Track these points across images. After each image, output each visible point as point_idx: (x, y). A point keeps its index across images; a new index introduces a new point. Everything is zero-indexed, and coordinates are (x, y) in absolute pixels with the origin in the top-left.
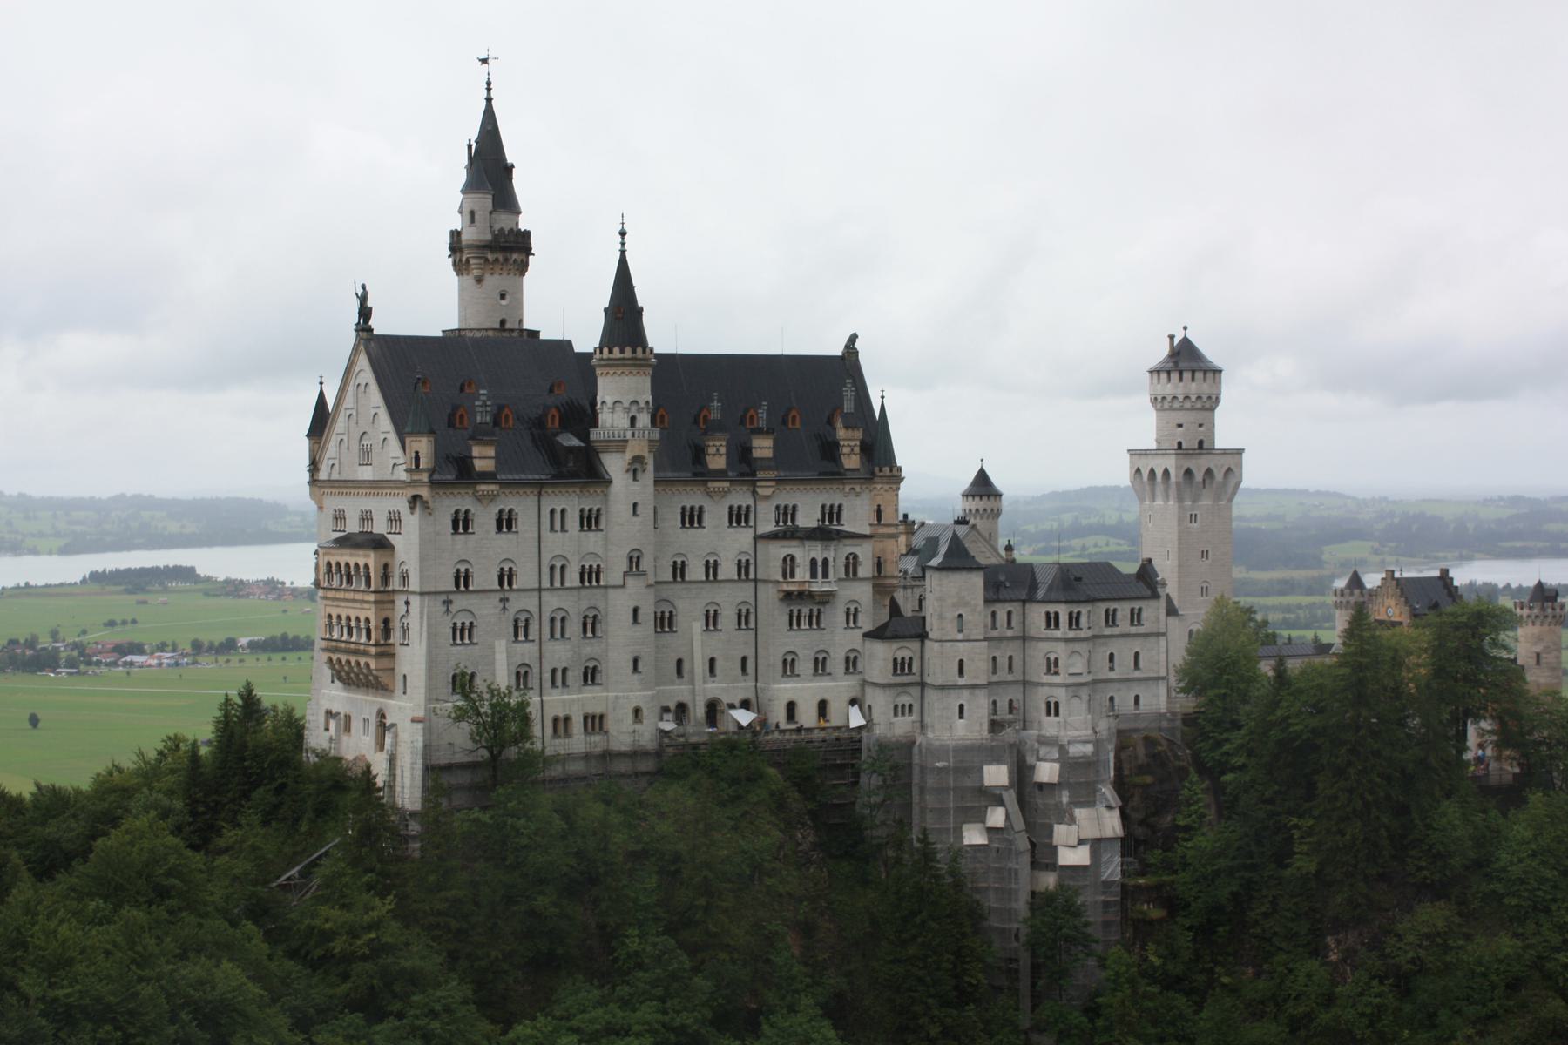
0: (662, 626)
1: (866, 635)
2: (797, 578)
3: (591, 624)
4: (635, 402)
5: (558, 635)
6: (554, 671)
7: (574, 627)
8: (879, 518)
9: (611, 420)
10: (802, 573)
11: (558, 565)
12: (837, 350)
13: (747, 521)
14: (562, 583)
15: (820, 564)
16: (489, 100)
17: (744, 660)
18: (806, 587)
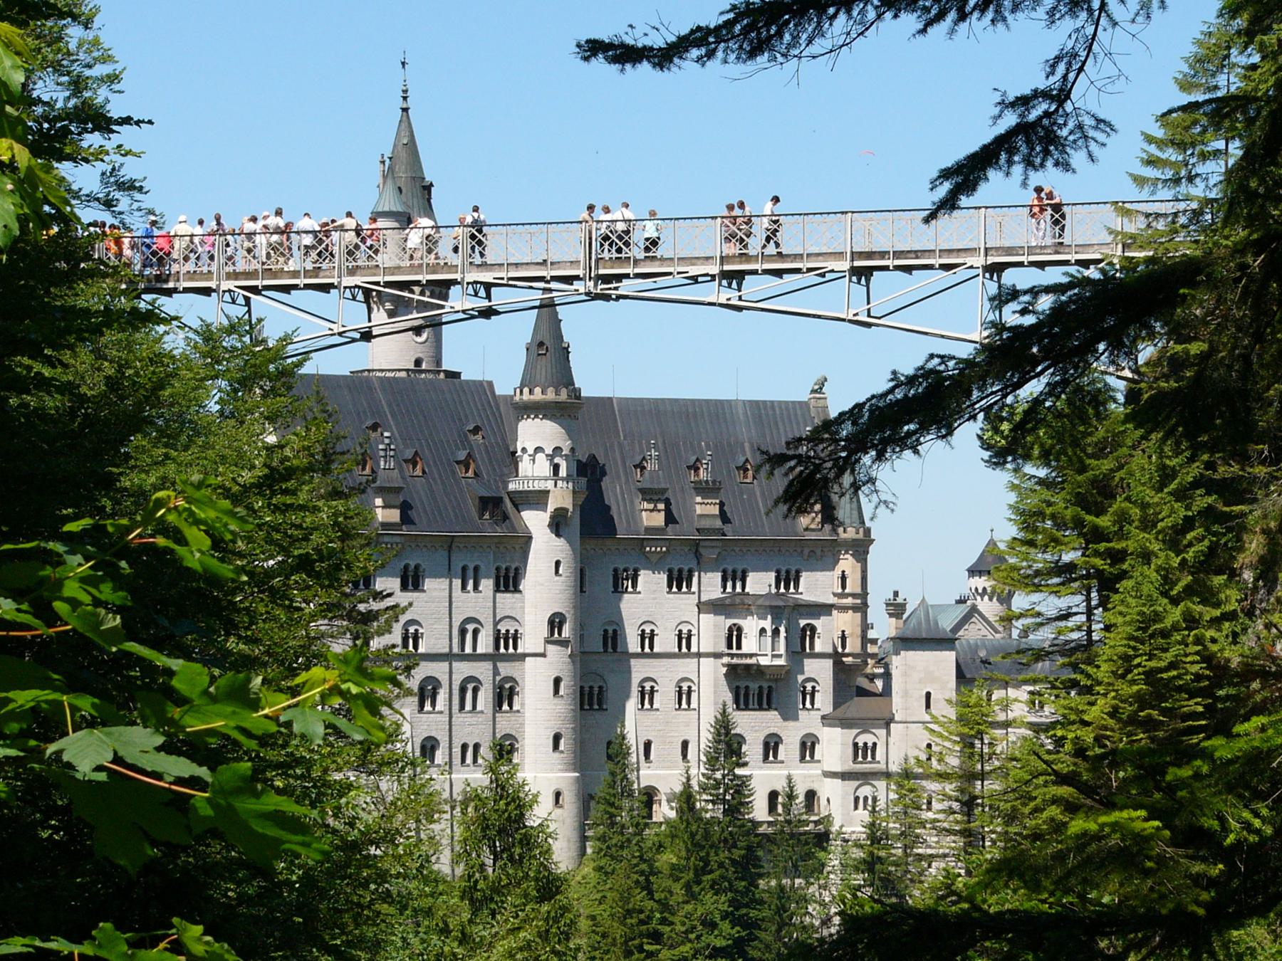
0: (591, 704)
1: (823, 717)
2: (745, 650)
3: (505, 694)
4: (557, 450)
5: (468, 707)
6: (464, 747)
7: (485, 698)
8: (844, 587)
9: (533, 471)
10: (749, 645)
11: (470, 627)
12: (804, 396)
13: (689, 586)
14: (475, 648)
15: (769, 633)
16: (405, 110)
17: (685, 744)
18: (753, 661)
